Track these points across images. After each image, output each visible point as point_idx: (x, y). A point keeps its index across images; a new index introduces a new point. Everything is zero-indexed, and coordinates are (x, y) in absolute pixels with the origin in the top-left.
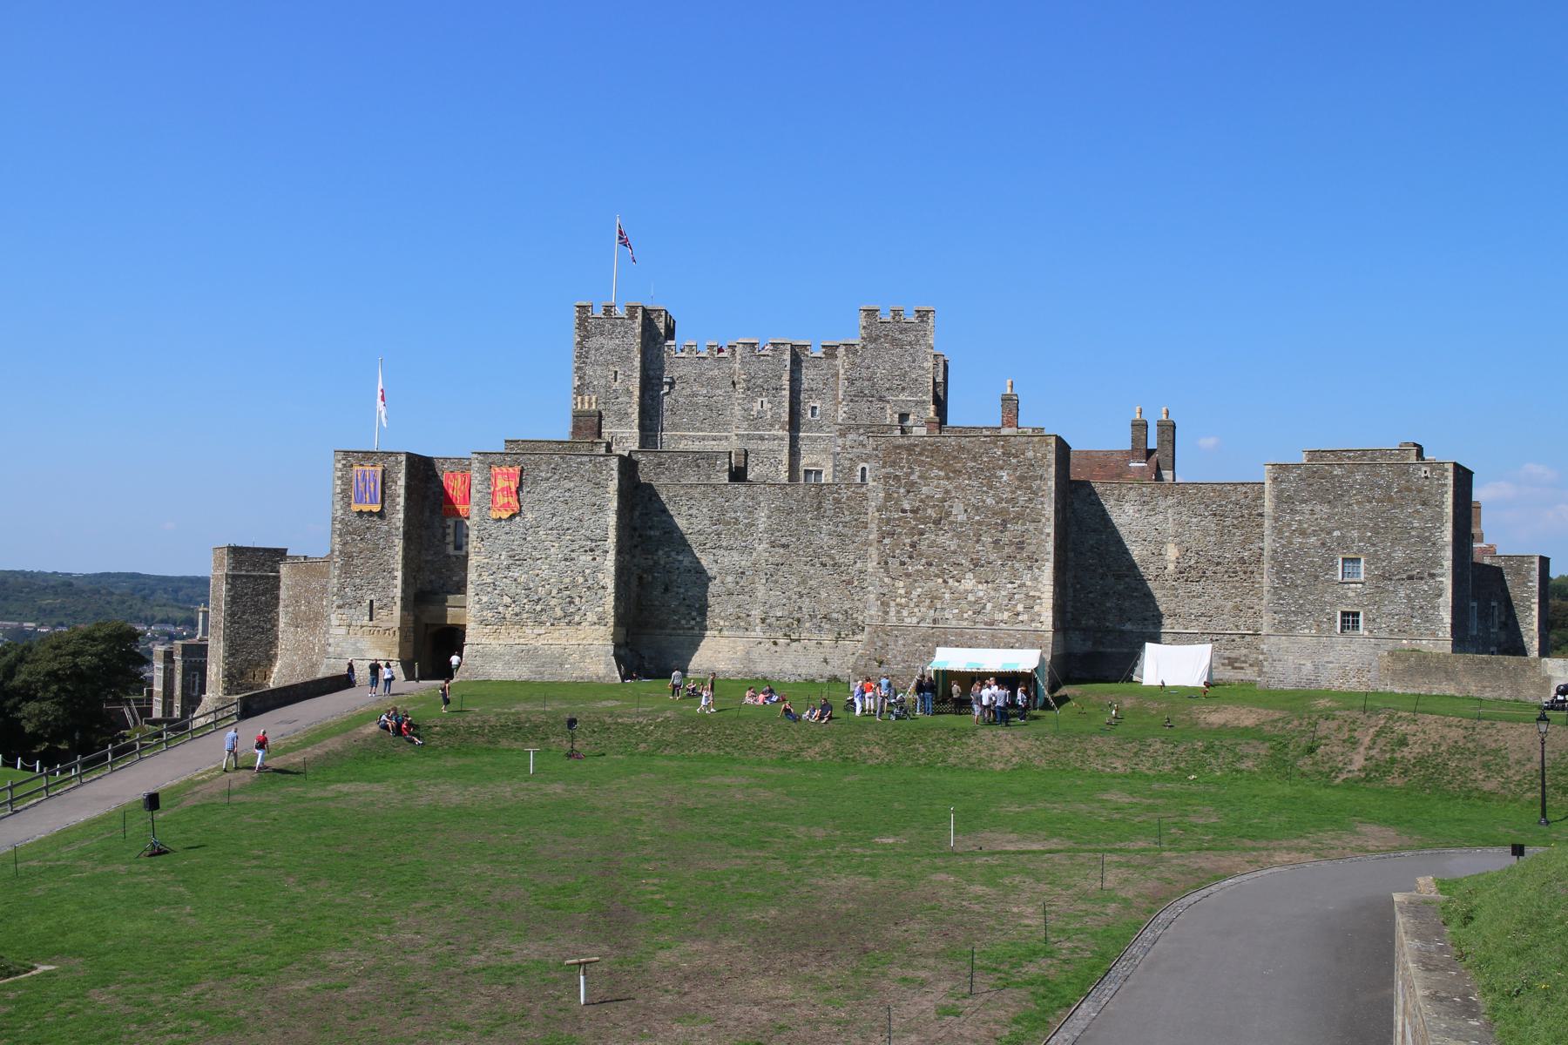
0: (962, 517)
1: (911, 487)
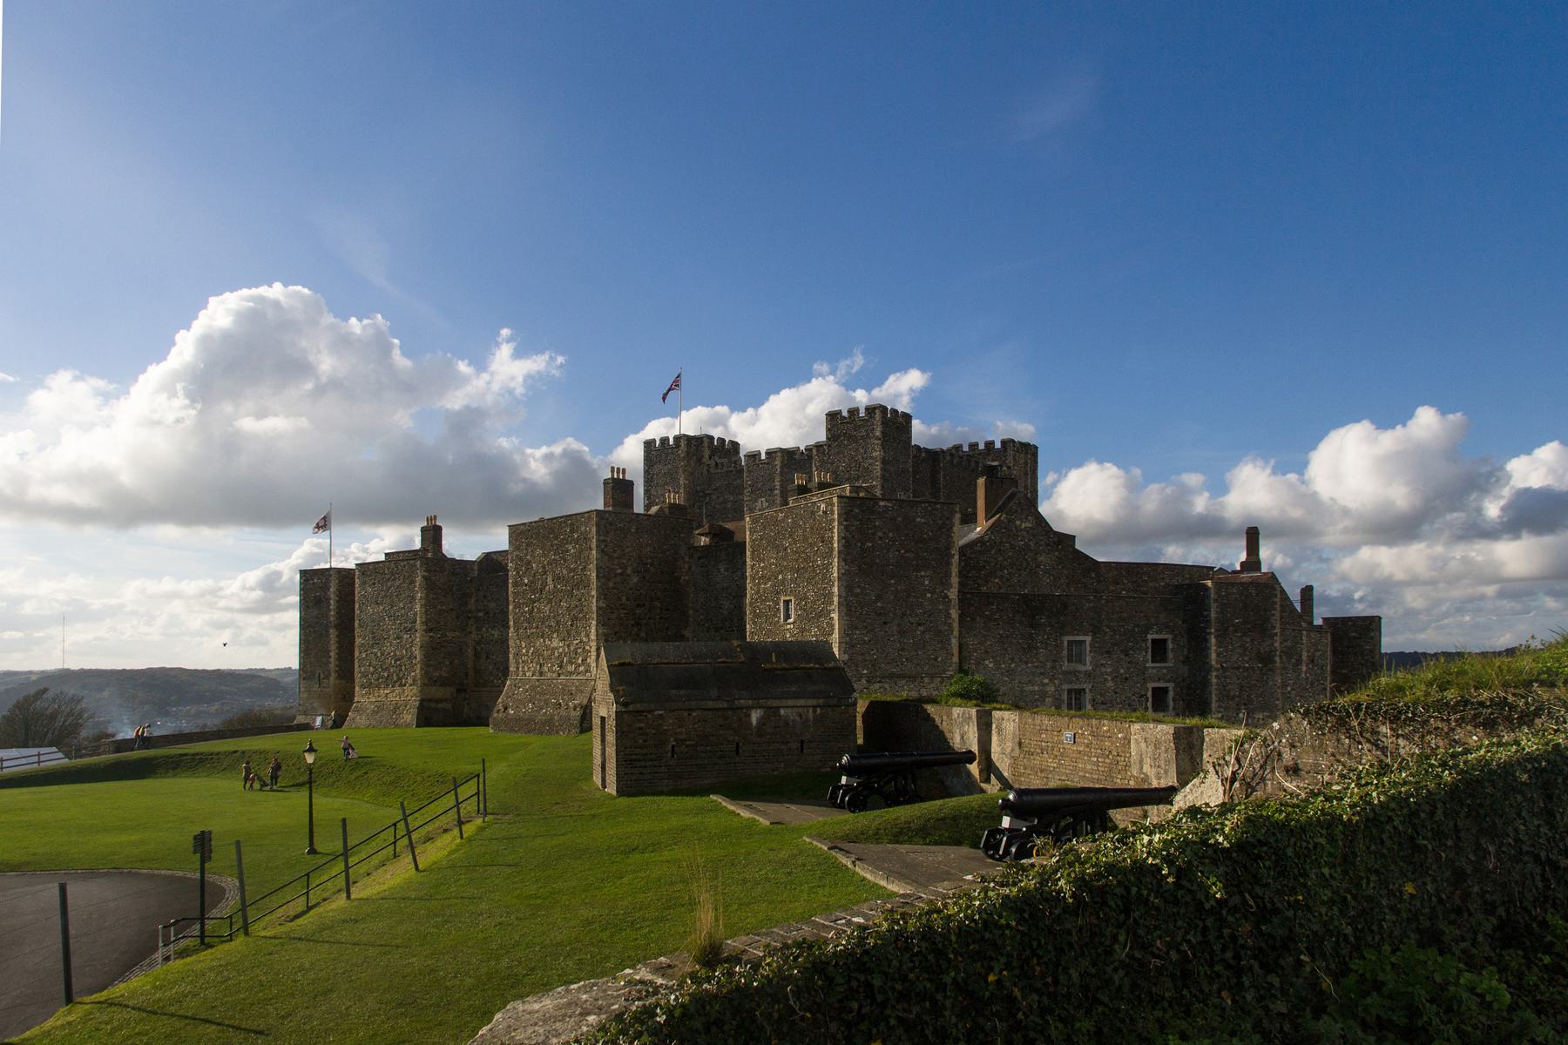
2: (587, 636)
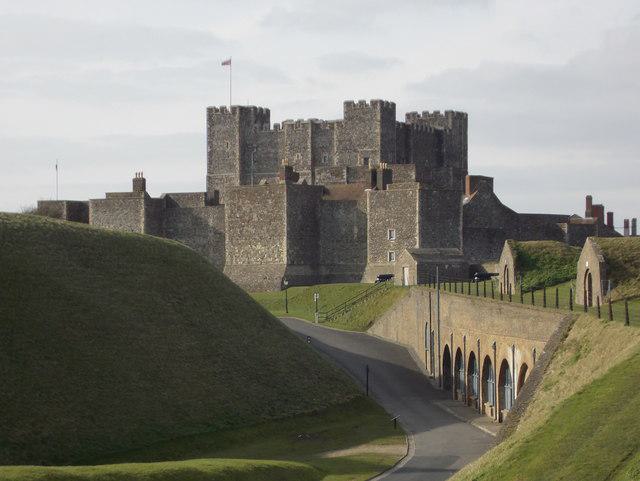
0: (256, 219)
1: (239, 208)
2: (281, 244)
